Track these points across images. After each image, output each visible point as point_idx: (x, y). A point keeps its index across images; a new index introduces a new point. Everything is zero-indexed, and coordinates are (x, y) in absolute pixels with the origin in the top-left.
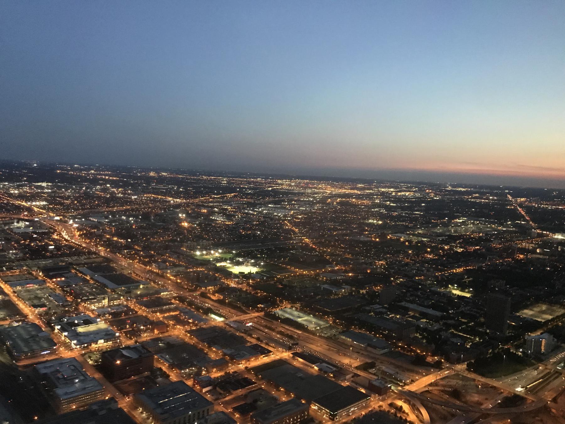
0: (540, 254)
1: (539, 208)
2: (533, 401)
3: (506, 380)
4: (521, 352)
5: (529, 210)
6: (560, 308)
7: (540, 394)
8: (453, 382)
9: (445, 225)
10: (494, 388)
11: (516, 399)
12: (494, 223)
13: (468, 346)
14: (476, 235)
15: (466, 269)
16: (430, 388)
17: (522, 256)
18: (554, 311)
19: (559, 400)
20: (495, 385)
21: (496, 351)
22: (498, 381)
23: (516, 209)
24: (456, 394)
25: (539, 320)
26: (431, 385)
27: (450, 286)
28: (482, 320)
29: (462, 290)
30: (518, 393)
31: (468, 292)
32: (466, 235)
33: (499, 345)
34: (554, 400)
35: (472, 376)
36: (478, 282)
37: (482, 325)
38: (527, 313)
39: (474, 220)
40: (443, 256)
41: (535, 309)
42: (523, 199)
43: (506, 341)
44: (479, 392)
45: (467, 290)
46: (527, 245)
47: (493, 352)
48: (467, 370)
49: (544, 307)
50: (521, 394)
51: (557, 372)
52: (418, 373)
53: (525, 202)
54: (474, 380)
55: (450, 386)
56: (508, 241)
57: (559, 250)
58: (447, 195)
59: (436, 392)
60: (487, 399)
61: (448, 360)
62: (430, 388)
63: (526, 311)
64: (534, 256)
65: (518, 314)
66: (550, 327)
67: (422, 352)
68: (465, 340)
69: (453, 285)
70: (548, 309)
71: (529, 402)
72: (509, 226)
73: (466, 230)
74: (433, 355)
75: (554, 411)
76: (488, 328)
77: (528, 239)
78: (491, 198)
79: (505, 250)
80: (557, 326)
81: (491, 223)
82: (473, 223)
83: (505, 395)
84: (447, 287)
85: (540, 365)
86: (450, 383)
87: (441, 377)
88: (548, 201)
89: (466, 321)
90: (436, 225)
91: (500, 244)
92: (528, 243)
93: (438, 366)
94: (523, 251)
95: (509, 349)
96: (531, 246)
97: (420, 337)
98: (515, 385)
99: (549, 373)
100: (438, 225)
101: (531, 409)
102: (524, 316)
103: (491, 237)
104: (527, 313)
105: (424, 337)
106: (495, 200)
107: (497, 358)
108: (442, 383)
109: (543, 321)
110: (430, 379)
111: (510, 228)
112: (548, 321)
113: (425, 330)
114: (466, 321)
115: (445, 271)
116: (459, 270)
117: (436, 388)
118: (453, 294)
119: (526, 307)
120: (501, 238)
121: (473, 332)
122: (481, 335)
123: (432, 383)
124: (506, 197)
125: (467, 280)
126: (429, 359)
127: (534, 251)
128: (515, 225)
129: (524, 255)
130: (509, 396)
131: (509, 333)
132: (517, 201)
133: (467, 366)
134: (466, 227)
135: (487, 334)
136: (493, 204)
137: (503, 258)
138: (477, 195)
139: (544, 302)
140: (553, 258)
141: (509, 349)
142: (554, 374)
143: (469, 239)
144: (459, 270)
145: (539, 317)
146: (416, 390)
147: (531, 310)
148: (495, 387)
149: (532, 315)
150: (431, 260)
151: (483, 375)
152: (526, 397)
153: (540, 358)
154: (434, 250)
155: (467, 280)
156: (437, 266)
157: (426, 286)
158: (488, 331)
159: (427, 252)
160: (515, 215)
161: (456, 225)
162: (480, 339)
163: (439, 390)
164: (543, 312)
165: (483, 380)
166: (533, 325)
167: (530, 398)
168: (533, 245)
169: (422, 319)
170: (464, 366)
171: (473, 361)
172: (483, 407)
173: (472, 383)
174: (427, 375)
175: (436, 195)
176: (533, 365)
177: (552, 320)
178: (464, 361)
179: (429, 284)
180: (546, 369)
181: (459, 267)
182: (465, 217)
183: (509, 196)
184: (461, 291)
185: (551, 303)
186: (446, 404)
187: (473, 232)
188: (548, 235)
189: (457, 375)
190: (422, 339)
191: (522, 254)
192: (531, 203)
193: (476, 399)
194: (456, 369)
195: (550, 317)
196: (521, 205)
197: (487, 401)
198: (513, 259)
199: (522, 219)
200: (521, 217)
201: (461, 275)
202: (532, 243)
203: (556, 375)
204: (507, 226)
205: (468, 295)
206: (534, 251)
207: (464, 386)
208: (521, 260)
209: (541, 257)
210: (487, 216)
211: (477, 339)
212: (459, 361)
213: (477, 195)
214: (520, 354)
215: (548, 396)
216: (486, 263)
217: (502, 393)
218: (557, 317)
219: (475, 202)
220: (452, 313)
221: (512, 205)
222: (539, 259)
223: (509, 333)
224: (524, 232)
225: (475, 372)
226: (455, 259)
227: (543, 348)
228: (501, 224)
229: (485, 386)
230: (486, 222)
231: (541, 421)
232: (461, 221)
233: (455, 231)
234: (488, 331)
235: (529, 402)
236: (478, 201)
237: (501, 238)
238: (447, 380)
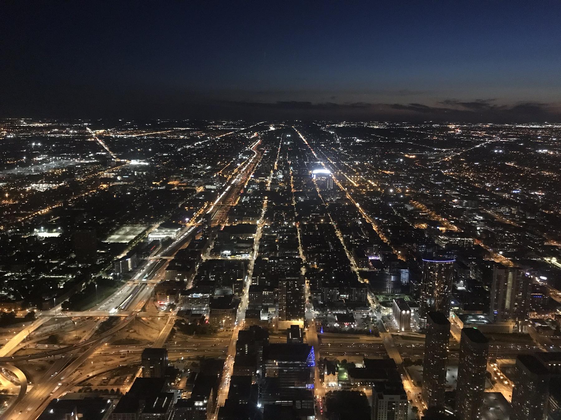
0: (120, 181)
1: (116, 138)
2: (126, 317)
3: (101, 307)
4: (112, 276)
5: (107, 140)
6: (141, 226)
7: (133, 309)
8: (50, 328)
9: (22, 165)
10: (90, 318)
11: (113, 319)
12: (76, 157)
13: (62, 287)
14: (59, 172)
15: (53, 209)
16: (24, 345)
17: (105, 186)
18: (136, 230)
19: (147, 308)
20: (91, 315)
21: (89, 283)
22: (94, 310)
23: (96, 142)
24: (53, 339)
25: (124, 242)
26: (23, 341)
27: (35, 230)
28: (73, 256)
29: (50, 231)
30: (113, 315)
31: (56, 232)
32: (48, 173)
33: (91, 276)
34: (143, 309)
35: (69, 314)
36: (65, 219)
37: (72, 261)
38: (114, 238)
39: (56, 156)
40: (25, 199)
41: (120, 233)
42: (101, 131)
43: (97, 269)
44: (76, 329)
45: (55, 230)
46: (108, 174)
47: (87, 285)
48: (63, 311)
49: (128, 229)
50: (116, 315)
51: (143, 284)
52: (7, 334)
53: (103, 133)
54: (70, 318)
55: (46, 334)
56: (91, 174)
57: (136, 174)
58: (22, 132)
59: (32, 347)
60: (84, 332)
61: (40, 308)
62: (24, 345)
63: (113, 237)
64: (116, 183)
65: (106, 242)
66: (134, 245)
67: (10, 309)
68: (56, 282)
69: (39, 228)
70: (131, 230)
71: (123, 319)
72: (91, 159)
73: (48, 168)
74: (23, 309)
75: (144, 319)
76: (79, 263)
77: (109, 169)
78: (71, 131)
79: (89, 182)
80: (140, 243)
81: (72, 157)
82: (55, 160)
83: (102, 320)
84: (32, 231)
85: (129, 282)
86: (44, 332)
87: (35, 328)
88: (123, 131)
89: (56, 262)
90: (12, 166)
91: (84, 177)
92: (109, 172)
93: (30, 318)
94: (106, 180)
95: (101, 277)
96: (112, 175)
97: (6, 294)
98: (108, 309)
99: (137, 286)
100: (16, 166)
101: (126, 324)
102: (112, 242)
103: (74, 172)
104: (114, 238)
105: (10, 293)
106: (75, 134)
107: (90, 288)
108: (38, 333)
109: (128, 242)
110: (23, 334)
111: (92, 160)
112: (132, 241)
113: (12, 283)
114: (56, 262)
115: (28, 215)
116: (44, 211)
117: (31, 342)
118: (41, 238)
119: (112, 233)
120: (85, 171)
121: (65, 271)
122: (72, 271)
123: (24, 339)
124: (86, 129)
125: (53, 219)
126: (20, 314)
127: (115, 180)
128: (96, 157)
129: (107, 184)
130: (105, 320)
131: (100, 261)
132: (95, 133)
133: (62, 307)
134: (48, 165)
135: (79, 269)
136: (74, 138)
137: (88, 191)
138: (56, 130)
139: (127, 224)
140: (132, 183)
141: (101, 277)
142: (141, 287)
143: (51, 177)
144: (44, 211)
145: (123, 239)
146: (7, 354)
147: (117, 234)
148: (91, 317)
149: (119, 239)
150: (11, 206)
151: (78, 310)
152: (120, 315)
153: (128, 276)
154: (14, 194)
155: (53, 219)
156: (18, 211)
157: (7, 235)
158: (80, 265)
159: (5, 198)
160: (95, 147)
161: (37, 163)
162: (72, 276)
163: (34, 343)
164: (127, 234)
165: (78, 314)
166: (118, 247)
167: (124, 315)
168: (114, 174)
169: (6, 273)
170: (60, 308)
171: (67, 300)
172: (81, 341)
173: (69, 322)
174: (18, 332)
175: (9, 133)
176: (123, 284)
177: (136, 239)
178: (57, 304)
179: (12, 233)
180: (134, 284)
181: (44, 208)
182: (45, 154)
183: (88, 129)
184: (49, 232)
185: (134, 223)
186: (45, 353)
187: (55, 169)
188: (125, 163)
189: (54, 320)
190: (9, 295)
191: (104, 184)
192: (109, 133)
193: (75, 336)
194: (51, 314)
195: (133, 237)
196: (100, 137)
197: (84, 334)
198: (98, 190)
199: (102, 151)
200: (101, 148)
201: (47, 216)
202: (113, 172)
203: (144, 285)
204: (89, 158)
205: (56, 235)
206: (115, 180)
207: (61, 327)
208: (105, 189)
209: (122, 183)
210: (68, 151)
211: (70, 277)
212: (53, 305)
213: (56, 130)
214: (111, 278)
215: (137, 308)
216: (72, 198)
217: (98, 320)
218: (140, 235)
219: (54, 138)
220: (42, 258)
221: (92, 137)
222: (119, 185)
223: (100, 261)
224: (105, 162)
225: (70, 310)
226: (38, 200)
227: (130, 266)
228: (83, 157)
229: (83, 319)
230: (68, 156)
231: (135, 331)
232: (41, 159)
233: (36, 171)
234: (80, 265)
235: (123, 319)
236: (58, 136)
237: (85, 171)
238: (42, 329)
